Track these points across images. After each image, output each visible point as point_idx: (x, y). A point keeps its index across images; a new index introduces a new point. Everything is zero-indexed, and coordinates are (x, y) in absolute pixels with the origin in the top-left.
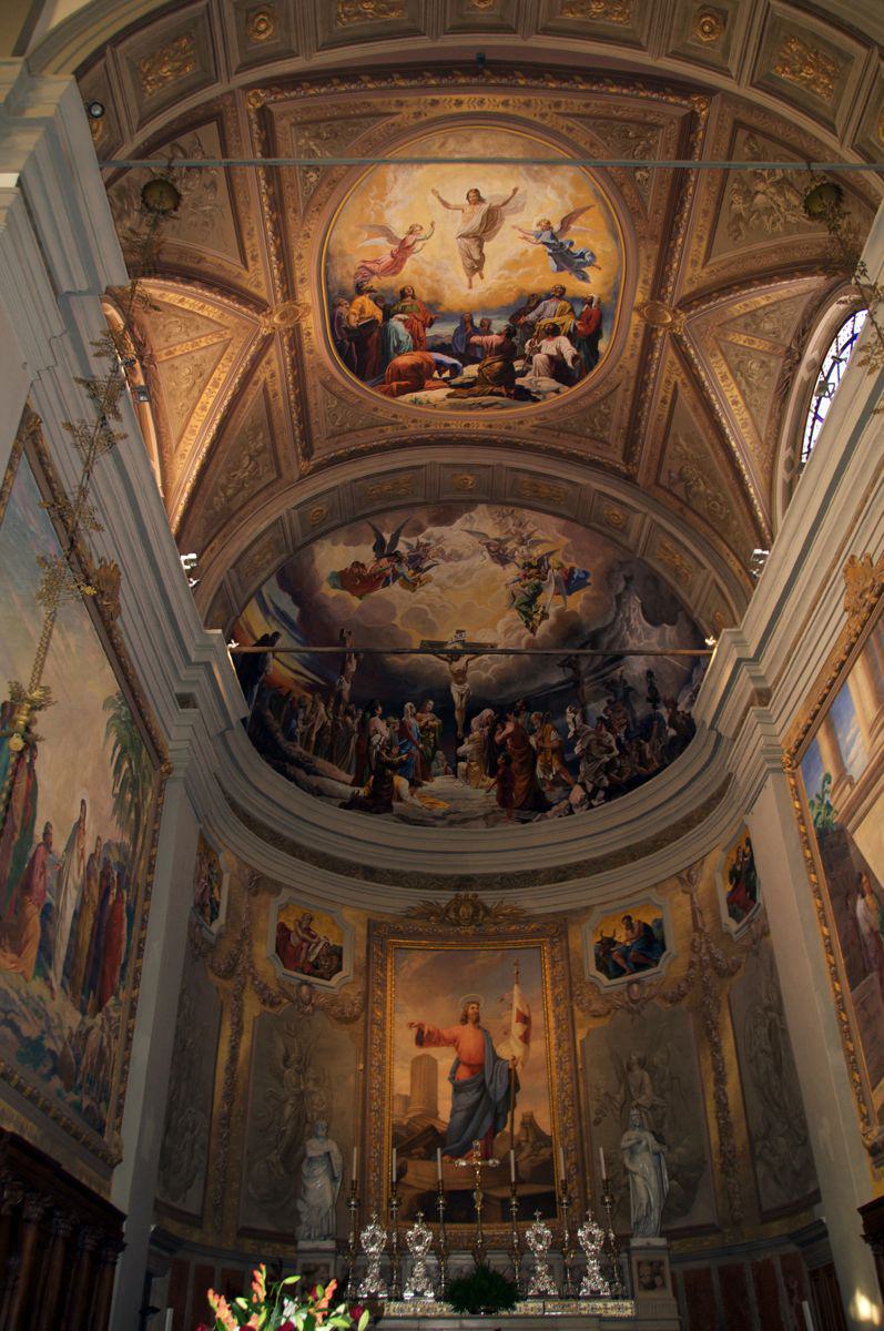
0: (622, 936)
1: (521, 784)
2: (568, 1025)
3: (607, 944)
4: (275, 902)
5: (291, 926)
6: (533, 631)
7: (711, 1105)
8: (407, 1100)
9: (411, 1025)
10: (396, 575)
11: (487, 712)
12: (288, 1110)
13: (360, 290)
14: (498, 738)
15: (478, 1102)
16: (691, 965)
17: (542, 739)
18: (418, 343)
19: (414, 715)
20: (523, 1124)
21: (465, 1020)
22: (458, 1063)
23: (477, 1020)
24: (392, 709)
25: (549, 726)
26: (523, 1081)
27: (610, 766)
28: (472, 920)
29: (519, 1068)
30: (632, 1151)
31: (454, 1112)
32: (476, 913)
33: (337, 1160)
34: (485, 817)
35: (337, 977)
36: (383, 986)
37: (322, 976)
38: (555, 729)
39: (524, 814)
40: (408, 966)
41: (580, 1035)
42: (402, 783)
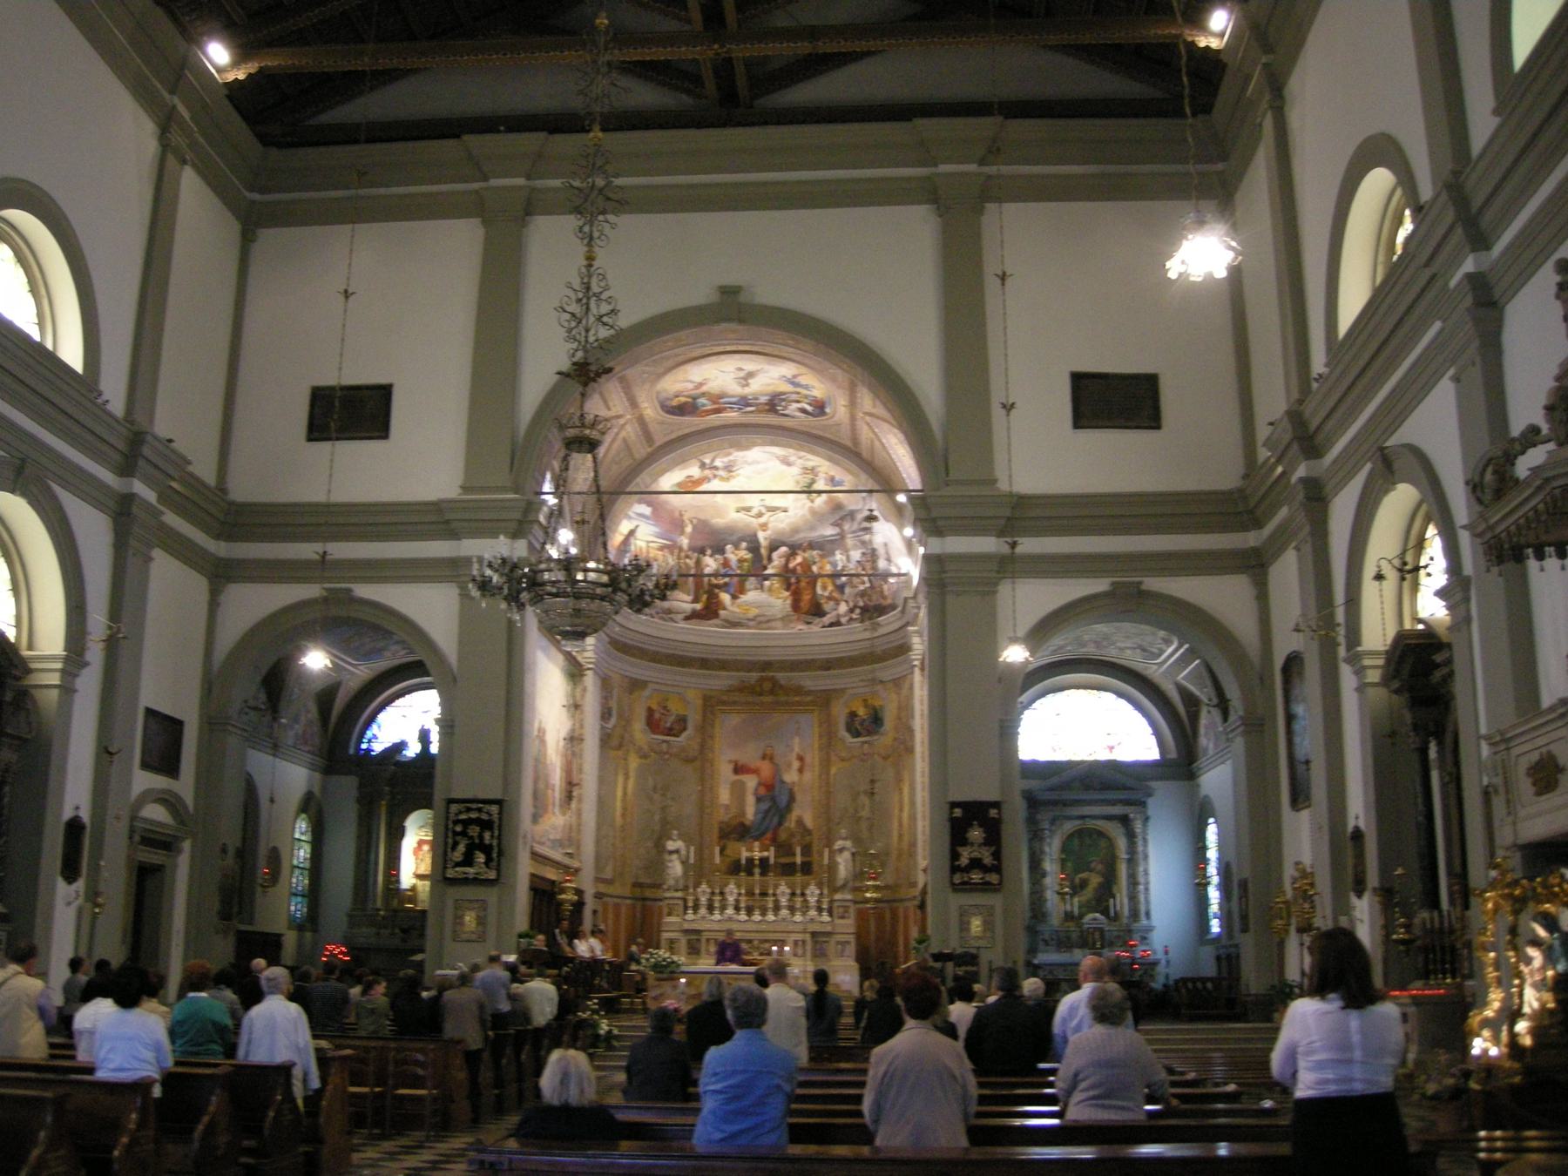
0: (861, 712)
1: (806, 597)
2: (826, 763)
3: (853, 715)
4: (647, 693)
5: (654, 707)
6: (812, 501)
7: (896, 825)
8: (727, 807)
9: (730, 761)
10: (715, 476)
11: (783, 549)
12: (657, 817)
13: (677, 396)
14: (791, 565)
15: (770, 809)
16: (895, 739)
17: (821, 568)
18: (714, 403)
19: (733, 553)
20: (797, 822)
21: (764, 757)
22: (760, 784)
23: (771, 759)
24: (719, 550)
25: (825, 560)
26: (799, 797)
27: (863, 594)
28: (772, 692)
29: (796, 789)
30: (841, 850)
31: (756, 814)
32: (774, 686)
33: (683, 852)
34: (782, 619)
35: (685, 735)
36: (712, 737)
37: (674, 735)
38: (830, 563)
39: (809, 618)
40: (729, 722)
41: (833, 770)
42: (725, 597)
